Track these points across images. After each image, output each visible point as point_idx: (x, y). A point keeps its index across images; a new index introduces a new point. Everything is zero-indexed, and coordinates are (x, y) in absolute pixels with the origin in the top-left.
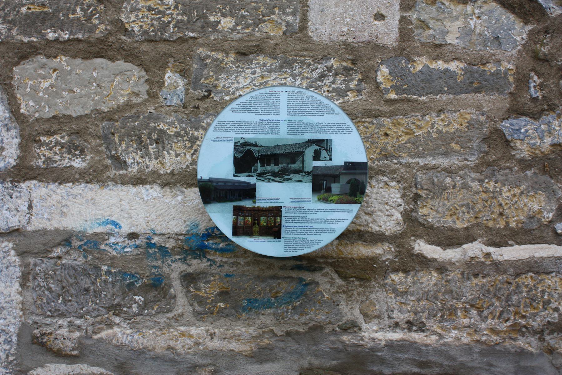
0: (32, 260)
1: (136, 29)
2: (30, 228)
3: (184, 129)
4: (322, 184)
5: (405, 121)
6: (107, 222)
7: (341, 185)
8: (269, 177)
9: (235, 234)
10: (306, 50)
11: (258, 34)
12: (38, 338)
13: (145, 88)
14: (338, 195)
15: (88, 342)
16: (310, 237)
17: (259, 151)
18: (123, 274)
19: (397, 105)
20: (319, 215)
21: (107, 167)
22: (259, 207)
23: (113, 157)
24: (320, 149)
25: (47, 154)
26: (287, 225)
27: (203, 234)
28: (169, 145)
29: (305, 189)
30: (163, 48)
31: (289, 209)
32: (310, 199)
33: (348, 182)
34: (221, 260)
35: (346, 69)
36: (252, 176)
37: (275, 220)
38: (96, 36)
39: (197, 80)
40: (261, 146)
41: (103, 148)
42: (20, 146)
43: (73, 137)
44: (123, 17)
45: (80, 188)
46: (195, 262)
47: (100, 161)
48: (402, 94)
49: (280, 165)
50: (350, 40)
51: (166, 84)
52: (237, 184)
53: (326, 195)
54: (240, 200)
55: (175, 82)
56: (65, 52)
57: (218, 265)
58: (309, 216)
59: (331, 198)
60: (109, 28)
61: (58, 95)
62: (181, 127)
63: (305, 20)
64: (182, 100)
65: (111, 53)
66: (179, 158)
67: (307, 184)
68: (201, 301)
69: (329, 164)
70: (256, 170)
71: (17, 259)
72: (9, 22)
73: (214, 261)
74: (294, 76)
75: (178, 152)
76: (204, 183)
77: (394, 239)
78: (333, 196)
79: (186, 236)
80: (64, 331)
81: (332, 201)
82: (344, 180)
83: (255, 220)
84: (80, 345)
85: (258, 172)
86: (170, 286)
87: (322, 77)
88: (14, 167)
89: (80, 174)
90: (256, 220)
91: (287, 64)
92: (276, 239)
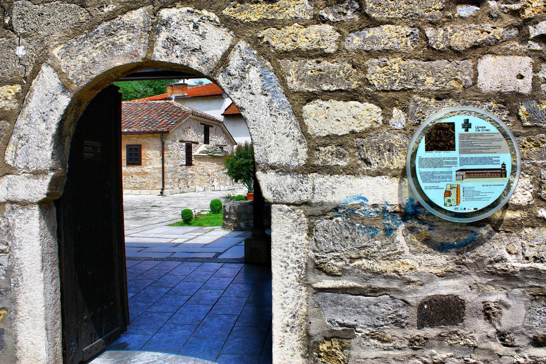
6: (360, 198)
10: (477, 96)
12: (318, 265)
13: (380, 119)
15: (348, 268)
21: (359, 165)
23: (362, 159)
30: (391, 95)
38: (353, 88)
42: (308, 153)
43: (339, 148)
44: (368, 76)
45: (342, 178)
47: (355, 161)
51: (394, 116)
60: (359, 83)
64: (404, 126)
65: (361, 98)
72: (301, 80)
77: (528, 207)
88: (304, 165)
89: (343, 170)
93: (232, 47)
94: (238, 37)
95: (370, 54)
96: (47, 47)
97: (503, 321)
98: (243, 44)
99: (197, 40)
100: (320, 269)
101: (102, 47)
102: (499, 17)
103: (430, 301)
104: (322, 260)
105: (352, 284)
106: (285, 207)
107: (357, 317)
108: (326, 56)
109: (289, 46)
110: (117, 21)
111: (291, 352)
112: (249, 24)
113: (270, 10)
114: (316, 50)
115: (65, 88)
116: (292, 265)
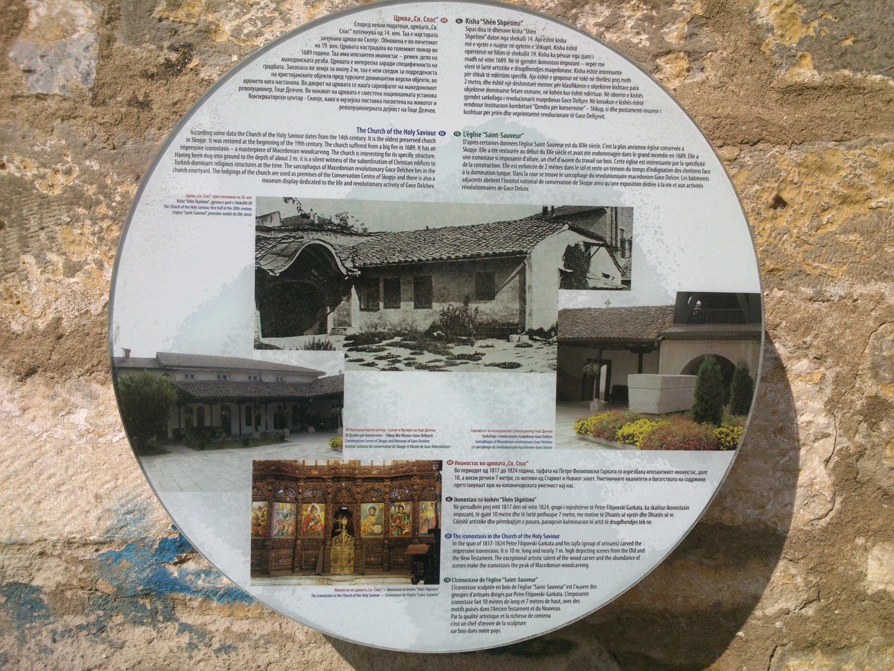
3: (90, 177)
4: (591, 373)
5: (844, 158)
7: (665, 381)
8: (395, 351)
14: (650, 416)
16: (546, 577)
17: (355, 251)
19: (819, 107)
20: (582, 494)
22: (354, 466)
24: (588, 246)
26: (461, 530)
27: (164, 541)
28: (42, 234)
29: (531, 392)
31: (471, 473)
32: (546, 435)
33: (691, 368)
34: (228, 629)
36: (326, 347)
37: (415, 512)
40: (365, 234)
46: (137, 634)
48: (836, 68)
49: (437, 306)
51: (33, 20)
52: (269, 379)
53: (607, 416)
54: (281, 439)
55: (64, 13)
57: (216, 645)
58: (547, 497)
59: (626, 430)
62: (85, 171)
66: (78, 278)
67: (537, 377)
69: (619, 300)
70: (344, 323)
73: (202, 634)
75: (75, 259)
76: (137, 375)
78: (633, 420)
79: (104, 550)
81: (629, 440)
82: (675, 359)
83: (339, 513)
85: (350, 331)
90: (344, 515)
92: (421, 585)
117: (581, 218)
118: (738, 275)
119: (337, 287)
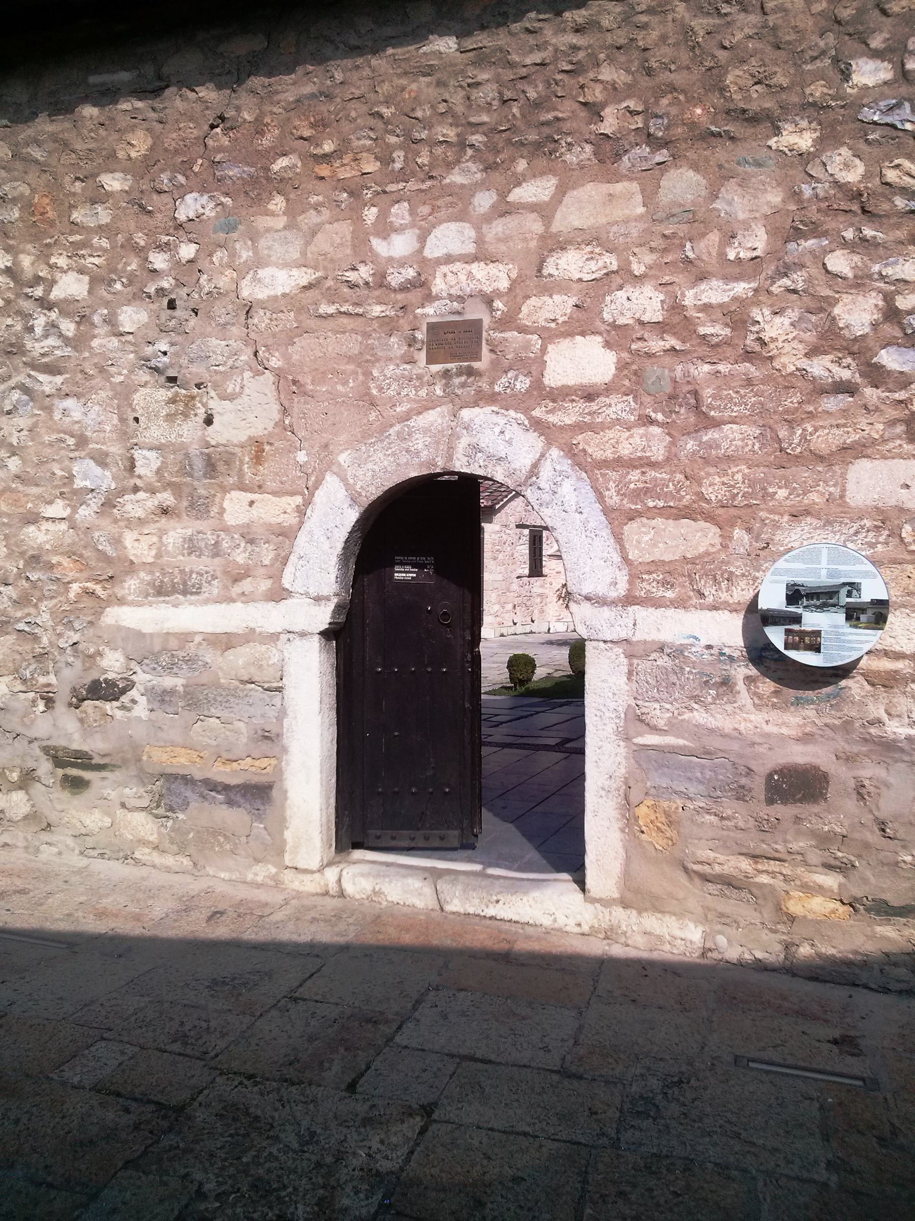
0: (635, 661)
1: (713, 498)
2: (634, 639)
4: (853, 614)
9: (786, 648)
11: (806, 502)
13: (718, 541)
15: (675, 721)
18: (701, 674)
20: (850, 638)
21: (690, 597)
25: (648, 587)
29: (841, 617)
30: (733, 512)
35: (876, 526)
39: (758, 535)
41: (687, 584)
42: (631, 582)
44: (703, 490)
45: (671, 612)
50: (880, 505)
56: (661, 515)
61: (655, 545)
63: (844, 490)
65: (694, 516)
68: (760, 697)
69: (858, 600)
71: (626, 661)
74: (834, 533)
80: (658, 712)
82: (870, 613)
84: (669, 723)
86: (736, 684)
87: (856, 533)
90: (802, 639)
91: (828, 523)
93: (543, 455)
94: (549, 443)
95: (706, 461)
96: (331, 453)
97: (882, 803)
98: (555, 452)
99: (502, 447)
100: (642, 721)
101: (393, 454)
102: (877, 409)
103: (781, 770)
104: (644, 710)
105: (681, 742)
106: (602, 644)
107: (688, 785)
108: (653, 465)
109: (609, 454)
110: (411, 423)
111: (607, 824)
112: (562, 428)
113: (587, 411)
114: (640, 458)
115: (354, 501)
116: (608, 714)
117: (851, 584)
118: (884, 596)
119: (802, 597)
